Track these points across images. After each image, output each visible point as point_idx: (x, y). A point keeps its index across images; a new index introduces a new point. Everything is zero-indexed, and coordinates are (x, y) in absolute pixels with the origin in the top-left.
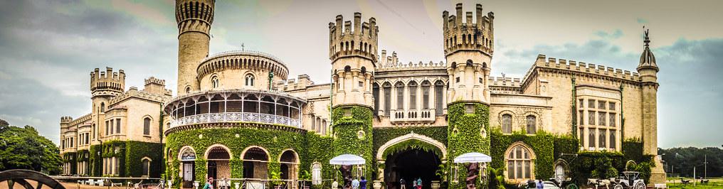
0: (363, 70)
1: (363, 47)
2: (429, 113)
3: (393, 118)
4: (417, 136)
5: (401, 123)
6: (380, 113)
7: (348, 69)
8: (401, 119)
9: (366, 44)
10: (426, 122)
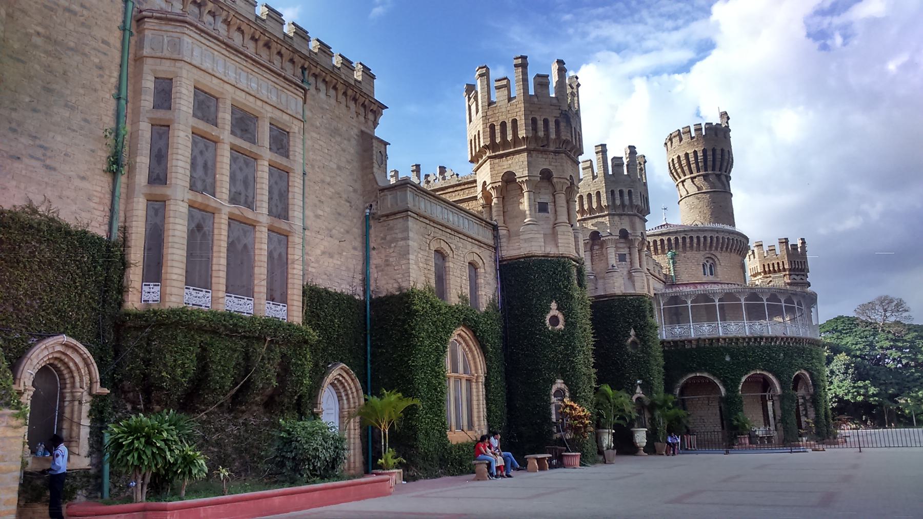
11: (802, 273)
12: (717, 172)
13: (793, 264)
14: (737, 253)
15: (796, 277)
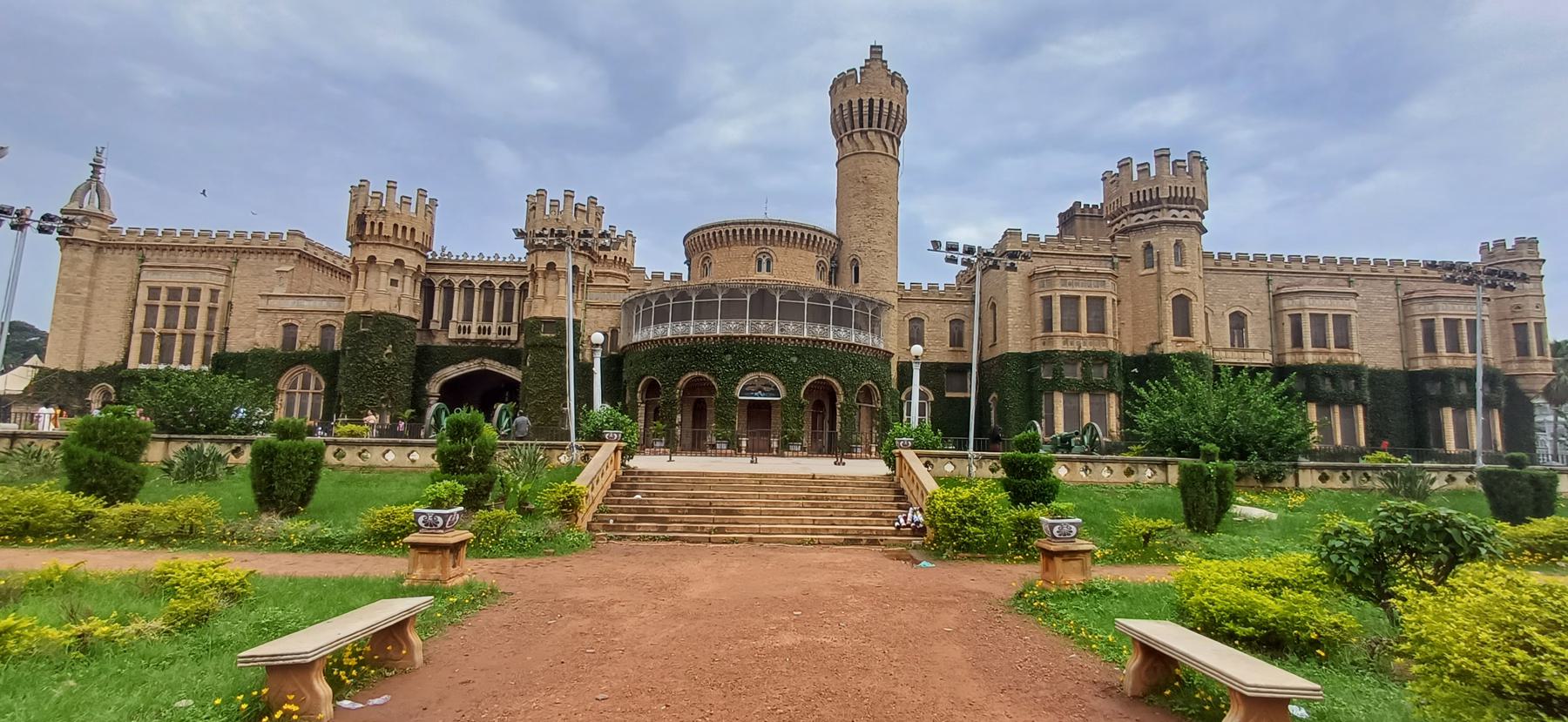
0: (399, 262)
2: (509, 328)
3: (453, 333)
4: (495, 366)
5: (465, 341)
6: (432, 326)
7: (372, 259)
8: (466, 336)
9: (404, 228)
11: (1155, 207)
12: (849, 132)
13: (1135, 201)
15: (1142, 216)
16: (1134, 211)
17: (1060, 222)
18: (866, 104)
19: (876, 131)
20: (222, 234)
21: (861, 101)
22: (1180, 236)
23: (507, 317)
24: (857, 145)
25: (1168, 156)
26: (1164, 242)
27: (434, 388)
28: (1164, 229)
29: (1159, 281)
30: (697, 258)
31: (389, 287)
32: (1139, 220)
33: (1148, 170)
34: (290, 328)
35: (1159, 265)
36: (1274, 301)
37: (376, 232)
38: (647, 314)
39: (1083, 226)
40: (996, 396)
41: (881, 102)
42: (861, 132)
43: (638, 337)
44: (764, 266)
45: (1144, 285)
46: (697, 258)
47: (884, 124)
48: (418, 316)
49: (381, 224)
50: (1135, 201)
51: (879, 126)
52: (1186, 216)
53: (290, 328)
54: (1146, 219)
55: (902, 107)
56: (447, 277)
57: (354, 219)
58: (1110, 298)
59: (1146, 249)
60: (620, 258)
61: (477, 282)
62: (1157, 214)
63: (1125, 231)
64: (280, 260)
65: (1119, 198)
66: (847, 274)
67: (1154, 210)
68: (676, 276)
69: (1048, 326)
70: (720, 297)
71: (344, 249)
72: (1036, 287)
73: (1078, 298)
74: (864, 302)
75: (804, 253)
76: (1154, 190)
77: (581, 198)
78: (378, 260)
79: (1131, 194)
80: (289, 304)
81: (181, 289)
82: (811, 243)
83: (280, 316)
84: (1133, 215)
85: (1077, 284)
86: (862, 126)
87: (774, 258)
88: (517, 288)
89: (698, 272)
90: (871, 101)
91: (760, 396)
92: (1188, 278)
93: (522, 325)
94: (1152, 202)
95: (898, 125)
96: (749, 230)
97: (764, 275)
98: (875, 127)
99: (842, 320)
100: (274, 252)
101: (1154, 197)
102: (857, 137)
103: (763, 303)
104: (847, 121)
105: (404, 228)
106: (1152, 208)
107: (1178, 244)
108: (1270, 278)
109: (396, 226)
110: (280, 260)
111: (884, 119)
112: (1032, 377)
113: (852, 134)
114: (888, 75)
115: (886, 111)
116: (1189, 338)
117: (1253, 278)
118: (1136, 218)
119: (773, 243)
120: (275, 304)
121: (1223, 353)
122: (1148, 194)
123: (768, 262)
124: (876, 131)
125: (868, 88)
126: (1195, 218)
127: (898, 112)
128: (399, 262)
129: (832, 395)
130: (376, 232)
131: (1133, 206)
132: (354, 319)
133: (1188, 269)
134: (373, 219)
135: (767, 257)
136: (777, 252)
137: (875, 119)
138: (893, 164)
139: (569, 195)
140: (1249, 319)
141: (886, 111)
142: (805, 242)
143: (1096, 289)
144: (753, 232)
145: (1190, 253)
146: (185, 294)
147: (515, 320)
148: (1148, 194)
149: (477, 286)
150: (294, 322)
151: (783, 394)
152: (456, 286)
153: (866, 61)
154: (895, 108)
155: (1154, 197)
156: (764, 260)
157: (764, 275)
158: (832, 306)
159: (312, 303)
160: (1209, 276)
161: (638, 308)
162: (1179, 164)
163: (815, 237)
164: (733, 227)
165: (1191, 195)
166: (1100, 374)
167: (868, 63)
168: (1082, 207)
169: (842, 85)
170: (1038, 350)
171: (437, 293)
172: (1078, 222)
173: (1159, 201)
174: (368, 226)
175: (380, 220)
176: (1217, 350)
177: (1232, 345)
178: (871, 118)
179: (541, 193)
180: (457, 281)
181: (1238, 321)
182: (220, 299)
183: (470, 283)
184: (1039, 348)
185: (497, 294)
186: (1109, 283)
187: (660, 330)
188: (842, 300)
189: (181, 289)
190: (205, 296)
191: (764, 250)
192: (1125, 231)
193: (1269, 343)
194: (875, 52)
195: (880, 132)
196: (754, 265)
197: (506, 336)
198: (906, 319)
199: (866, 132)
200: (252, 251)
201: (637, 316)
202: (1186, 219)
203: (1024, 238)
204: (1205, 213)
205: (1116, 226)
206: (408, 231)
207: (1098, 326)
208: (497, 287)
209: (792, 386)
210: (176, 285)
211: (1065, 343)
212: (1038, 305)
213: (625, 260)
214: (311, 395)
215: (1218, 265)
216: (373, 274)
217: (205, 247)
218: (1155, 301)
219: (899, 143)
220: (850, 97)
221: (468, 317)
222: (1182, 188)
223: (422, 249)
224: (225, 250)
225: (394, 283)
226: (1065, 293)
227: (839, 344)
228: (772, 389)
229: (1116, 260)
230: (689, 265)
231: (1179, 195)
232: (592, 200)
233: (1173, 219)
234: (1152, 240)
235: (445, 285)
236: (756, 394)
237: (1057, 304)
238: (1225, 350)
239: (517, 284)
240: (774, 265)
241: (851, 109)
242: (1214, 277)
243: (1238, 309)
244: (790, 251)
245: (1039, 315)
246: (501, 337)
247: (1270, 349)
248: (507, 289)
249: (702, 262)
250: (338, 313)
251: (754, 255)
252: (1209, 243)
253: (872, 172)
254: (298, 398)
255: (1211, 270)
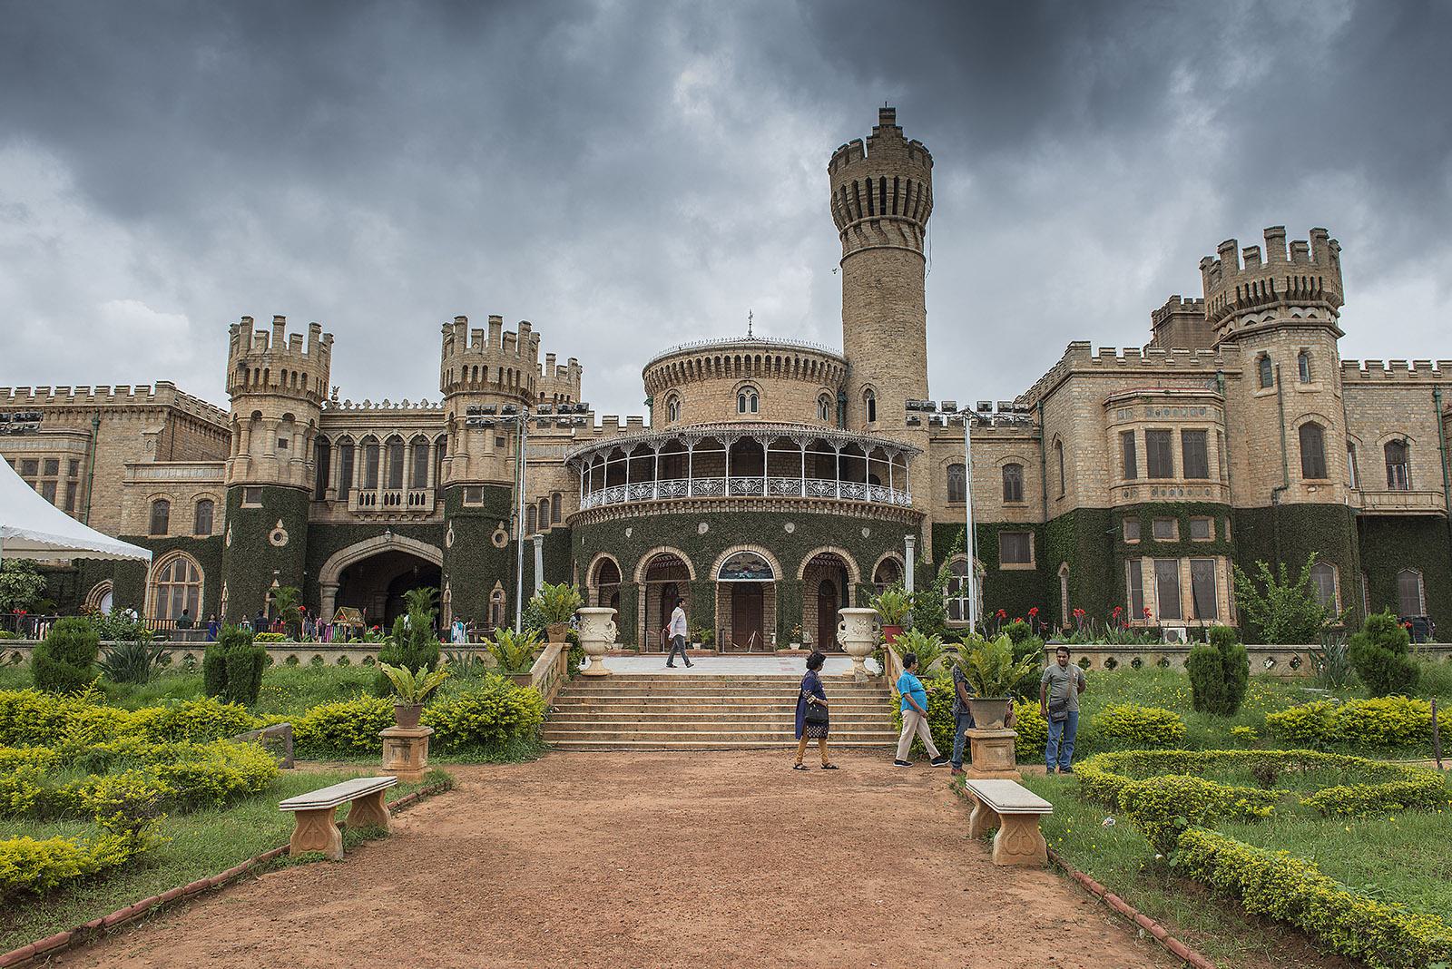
0: (289, 418)
1: (289, 379)
2: (423, 495)
5: (368, 514)
6: (329, 496)
7: (257, 416)
9: (294, 374)
10: (416, 514)
13: (1243, 297)
14: (748, 368)
15: (1254, 318)
16: (1244, 311)
17: (1155, 322)
18: (876, 185)
19: (890, 220)
20: (83, 391)
21: (869, 182)
22: (1305, 343)
23: (420, 482)
24: (866, 238)
25: (1283, 236)
26: (1282, 350)
27: (330, 572)
28: (1283, 334)
29: (1281, 404)
30: (660, 396)
31: (277, 450)
32: (1250, 322)
33: (1257, 257)
34: (161, 504)
35: (1279, 383)
36: (1444, 424)
37: (261, 381)
38: (598, 474)
39: (1185, 328)
40: (1067, 568)
41: (896, 181)
42: (872, 222)
43: (587, 503)
44: (748, 405)
45: (1260, 411)
46: (660, 396)
47: (901, 209)
48: (312, 485)
49: (267, 371)
50: (1243, 297)
51: (895, 213)
52: (1312, 316)
53: (161, 504)
54: (1259, 321)
55: (925, 186)
56: (345, 433)
57: (236, 365)
58: (1212, 429)
59: (1262, 361)
60: (562, 396)
61: (382, 437)
62: (1272, 314)
63: (1234, 338)
64: (147, 419)
65: (1222, 293)
66: (859, 410)
67: (1269, 309)
68: (635, 422)
69: (1130, 469)
70: (690, 449)
71: (223, 402)
72: (1113, 416)
73: (1169, 431)
74: (879, 451)
75: (802, 385)
76: (1267, 283)
77: (511, 325)
78: (264, 415)
79: (1238, 288)
80: (162, 474)
81: (36, 462)
82: (809, 372)
83: (149, 491)
84: (1243, 316)
85: (1167, 413)
86: (871, 213)
87: (761, 393)
88: (432, 443)
89: (662, 413)
90: (883, 181)
91: (746, 577)
92: (1319, 400)
93: (440, 493)
94: (1266, 299)
95: (921, 209)
96: (727, 359)
97: (748, 416)
98: (889, 214)
99: (851, 471)
100: (141, 410)
101: (1268, 291)
102: (866, 228)
103: (747, 456)
104: (852, 208)
105: (294, 374)
106: (1266, 306)
107: (1303, 353)
108: (1437, 393)
109: (284, 372)
110: (147, 419)
111: (901, 202)
112: (1112, 540)
113: (860, 224)
114: (904, 146)
115: (903, 192)
116: (1324, 481)
117: (1414, 394)
118: (1245, 320)
119: (758, 375)
120: (144, 475)
121: (1376, 499)
122: (1259, 288)
123: (754, 399)
124: (890, 220)
125: (879, 164)
126: (1324, 317)
127: (919, 192)
128: (289, 418)
129: (843, 572)
130: (261, 381)
131: (1241, 304)
132: (236, 491)
133: (1319, 387)
134: (258, 366)
135: (752, 392)
136: (766, 385)
137: (889, 203)
138: (916, 260)
139: (496, 322)
140: (1411, 451)
141: (903, 192)
142: (801, 370)
143: (1194, 419)
144: (732, 361)
145: (1319, 364)
146: (41, 467)
147: (430, 484)
148: (1259, 288)
149: (382, 443)
150: (166, 497)
151: (777, 574)
152: (357, 443)
153: (874, 129)
154: (915, 187)
155: (1268, 291)
156: (748, 397)
157: (748, 416)
158: (838, 454)
159: (193, 472)
160: (1354, 392)
161: (586, 467)
162: (1297, 247)
163: (814, 362)
164: (706, 355)
165: (1317, 288)
166: (1207, 532)
167: (877, 132)
168: (1183, 303)
169: (843, 160)
170: (1119, 503)
171: (333, 452)
172: (1177, 322)
173: (1275, 297)
174: (252, 374)
175: (266, 365)
176: (1369, 494)
177: (1390, 483)
178: (883, 202)
179: (462, 321)
180: (358, 437)
181: (1397, 451)
182: (80, 470)
183: (373, 438)
184: (1120, 501)
185: (407, 452)
186: (1210, 409)
187: (615, 495)
188: (851, 447)
189: (36, 462)
190: (63, 468)
191: (747, 383)
192: (1234, 338)
193: (1441, 481)
194: (886, 117)
195: (896, 220)
196: (735, 403)
197: (420, 507)
198: (944, 466)
199: (878, 221)
200: (115, 411)
201: (586, 476)
202: (1312, 320)
203: (1095, 353)
204: (1340, 309)
205: (1222, 331)
206: (299, 378)
207: (1195, 466)
208: (407, 443)
209: (789, 566)
210: (31, 456)
211: (1154, 493)
212: (1116, 444)
213: (568, 397)
214: (186, 588)
215: (1352, 378)
216: (259, 434)
217: (64, 407)
218: (1278, 432)
219: (923, 232)
220: (854, 177)
221: (372, 485)
222: (1304, 278)
223: (314, 399)
224: (86, 411)
225: (283, 443)
226: (1151, 426)
227: (849, 505)
228: (761, 567)
229: (1221, 377)
230: (651, 406)
231: (1301, 289)
232: (525, 326)
233: (1295, 320)
234: (1271, 350)
235: (343, 442)
236: (741, 574)
237: (1140, 441)
238: (1379, 493)
239: (431, 437)
240: (761, 403)
241: (857, 192)
242: (1360, 394)
243: (1395, 436)
244: (781, 383)
245: (1118, 455)
246: (414, 507)
247: (1442, 489)
248: (419, 444)
249: (668, 401)
250: (215, 484)
251: (735, 391)
252: (1347, 349)
253: (888, 273)
254: (171, 594)
255: (1356, 384)
